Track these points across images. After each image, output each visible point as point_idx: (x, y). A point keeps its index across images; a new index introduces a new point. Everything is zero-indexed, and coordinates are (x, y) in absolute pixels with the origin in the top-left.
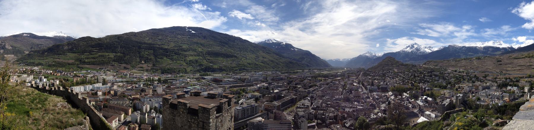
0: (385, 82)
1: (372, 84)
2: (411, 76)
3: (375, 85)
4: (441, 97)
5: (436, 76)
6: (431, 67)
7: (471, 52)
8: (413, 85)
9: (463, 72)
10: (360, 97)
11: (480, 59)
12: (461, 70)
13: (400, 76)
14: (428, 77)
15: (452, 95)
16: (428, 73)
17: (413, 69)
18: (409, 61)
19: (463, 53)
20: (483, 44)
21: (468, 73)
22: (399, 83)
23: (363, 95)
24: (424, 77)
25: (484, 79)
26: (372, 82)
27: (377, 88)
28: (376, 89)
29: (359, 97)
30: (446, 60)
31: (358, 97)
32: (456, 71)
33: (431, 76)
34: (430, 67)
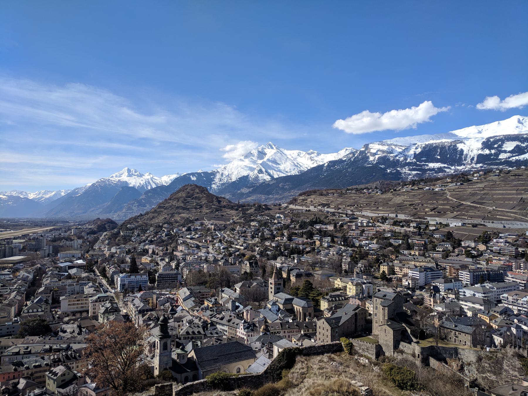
1: (134, 269)
3: (142, 270)
4: (335, 296)
5: (323, 234)
6: (312, 208)
7: (437, 161)
8: (254, 263)
9: (407, 223)
10: (87, 311)
11: (469, 180)
12: (402, 217)
13: (220, 241)
14: (302, 237)
15: (368, 293)
16: (301, 227)
17: (259, 218)
18: (249, 196)
19: (409, 164)
20: (480, 132)
21: (423, 226)
22: (216, 261)
23: (97, 304)
24: (290, 239)
25: (482, 247)
26: (133, 261)
27: (145, 277)
28: (146, 282)
29: (84, 315)
30: (352, 190)
31: (81, 312)
32: (384, 220)
33: (310, 235)
34: (308, 209)
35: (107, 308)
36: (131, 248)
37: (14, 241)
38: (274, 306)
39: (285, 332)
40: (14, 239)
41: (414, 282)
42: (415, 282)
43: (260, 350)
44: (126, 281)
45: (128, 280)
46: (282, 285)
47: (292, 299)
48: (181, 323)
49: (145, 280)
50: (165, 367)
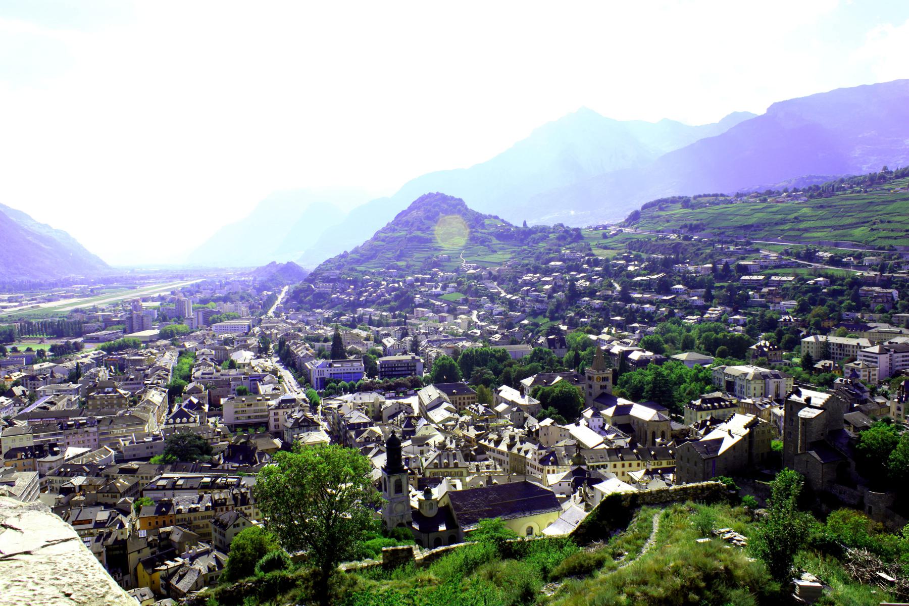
0: (405, 334)
2: (554, 290)
35: (297, 419)
36: (331, 314)
37: (145, 304)
38: (596, 420)
39: (615, 466)
40: (145, 300)
41: (867, 373)
42: (869, 372)
43: (569, 497)
44: (325, 372)
45: (329, 372)
46: (611, 381)
47: (630, 407)
48: (425, 448)
49: (359, 371)
50: (400, 521)
